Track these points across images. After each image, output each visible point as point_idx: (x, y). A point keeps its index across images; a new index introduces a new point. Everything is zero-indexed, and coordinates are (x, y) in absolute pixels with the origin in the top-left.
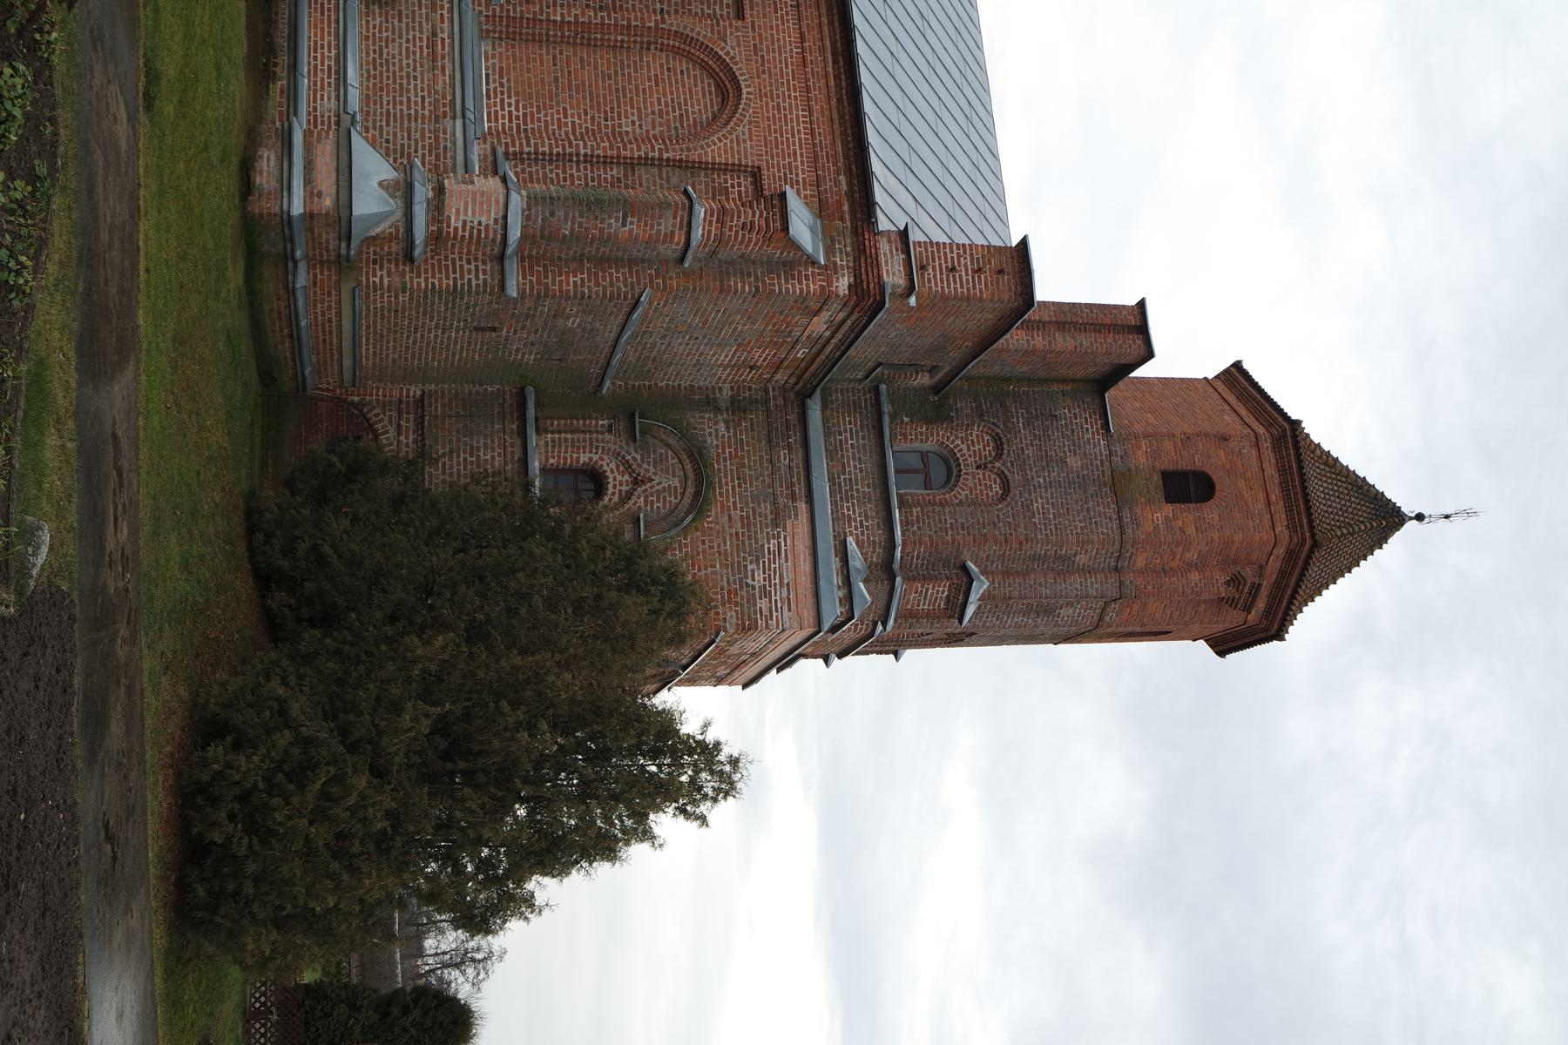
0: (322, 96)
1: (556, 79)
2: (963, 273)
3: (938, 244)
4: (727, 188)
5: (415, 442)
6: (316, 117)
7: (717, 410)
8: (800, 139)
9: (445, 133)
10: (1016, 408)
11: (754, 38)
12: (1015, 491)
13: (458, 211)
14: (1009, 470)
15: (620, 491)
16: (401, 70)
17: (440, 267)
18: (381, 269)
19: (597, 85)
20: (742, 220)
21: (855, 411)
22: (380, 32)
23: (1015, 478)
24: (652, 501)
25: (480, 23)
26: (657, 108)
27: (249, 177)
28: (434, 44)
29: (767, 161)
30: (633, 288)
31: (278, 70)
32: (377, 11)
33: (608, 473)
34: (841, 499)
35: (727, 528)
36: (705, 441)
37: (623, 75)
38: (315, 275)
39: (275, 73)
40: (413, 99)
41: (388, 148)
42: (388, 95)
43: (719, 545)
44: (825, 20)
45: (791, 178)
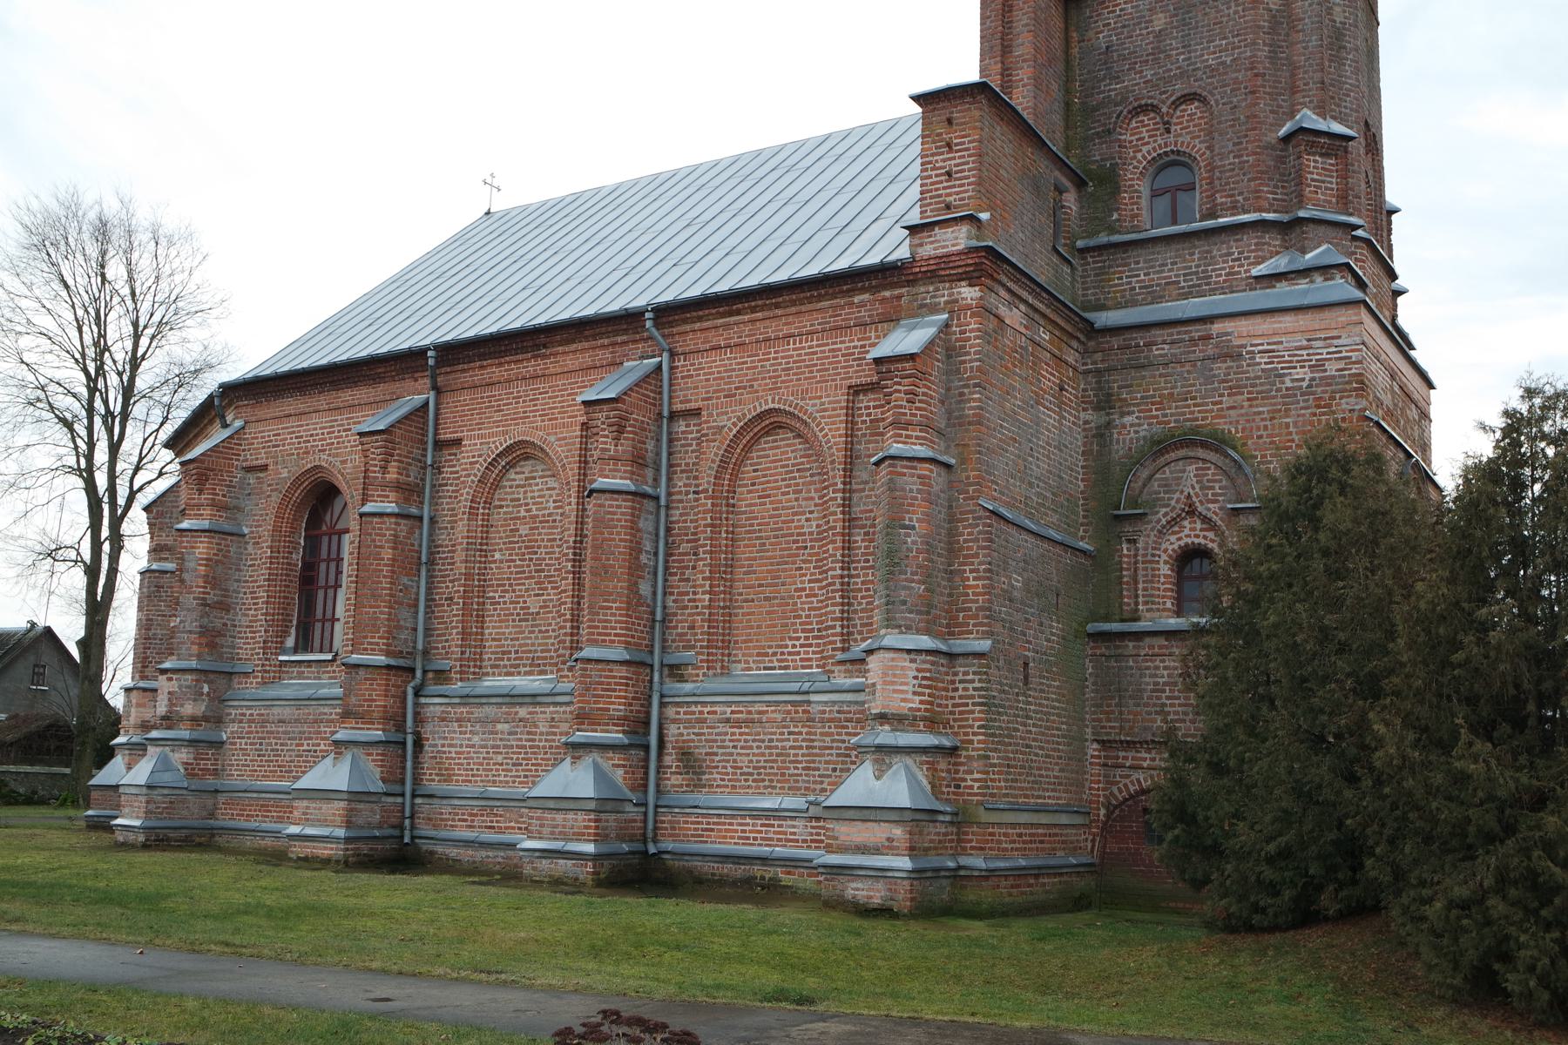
0: (792, 834)
1: (766, 599)
2: (953, 162)
3: (922, 193)
4: (871, 421)
5: (1149, 751)
6: (812, 841)
7: (1109, 424)
8: (818, 346)
9: (824, 712)
10: (1099, 93)
11: (718, 398)
12: (1195, 87)
13: (903, 700)
14: (1171, 96)
15: (1201, 530)
16: (763, 755)
17: (961, 720)
18: (965, 780)
19: (770, 558)
20: (905, 403)
21: (1107, 273)
22: (727, 774)
23: (1180, 88)
24: (1213, 495)
25: (715, 675)
26: (792, 496)
27: (875, 910)
29: (841, 379)
30: (980, 518)
31: (767, 876)
32: (707, 776)
33: (1182, 543)
34: (1207, 284)
35: (1243, 411)
36: (1145, 437)
37: (760, 531)
38: (972, 848)
39: (770, 879)
40: (791, 743)
41: (841, 770)
42: (789, 768)
43: (1262, 420)
44: (697, 326)
45: (859, 353)
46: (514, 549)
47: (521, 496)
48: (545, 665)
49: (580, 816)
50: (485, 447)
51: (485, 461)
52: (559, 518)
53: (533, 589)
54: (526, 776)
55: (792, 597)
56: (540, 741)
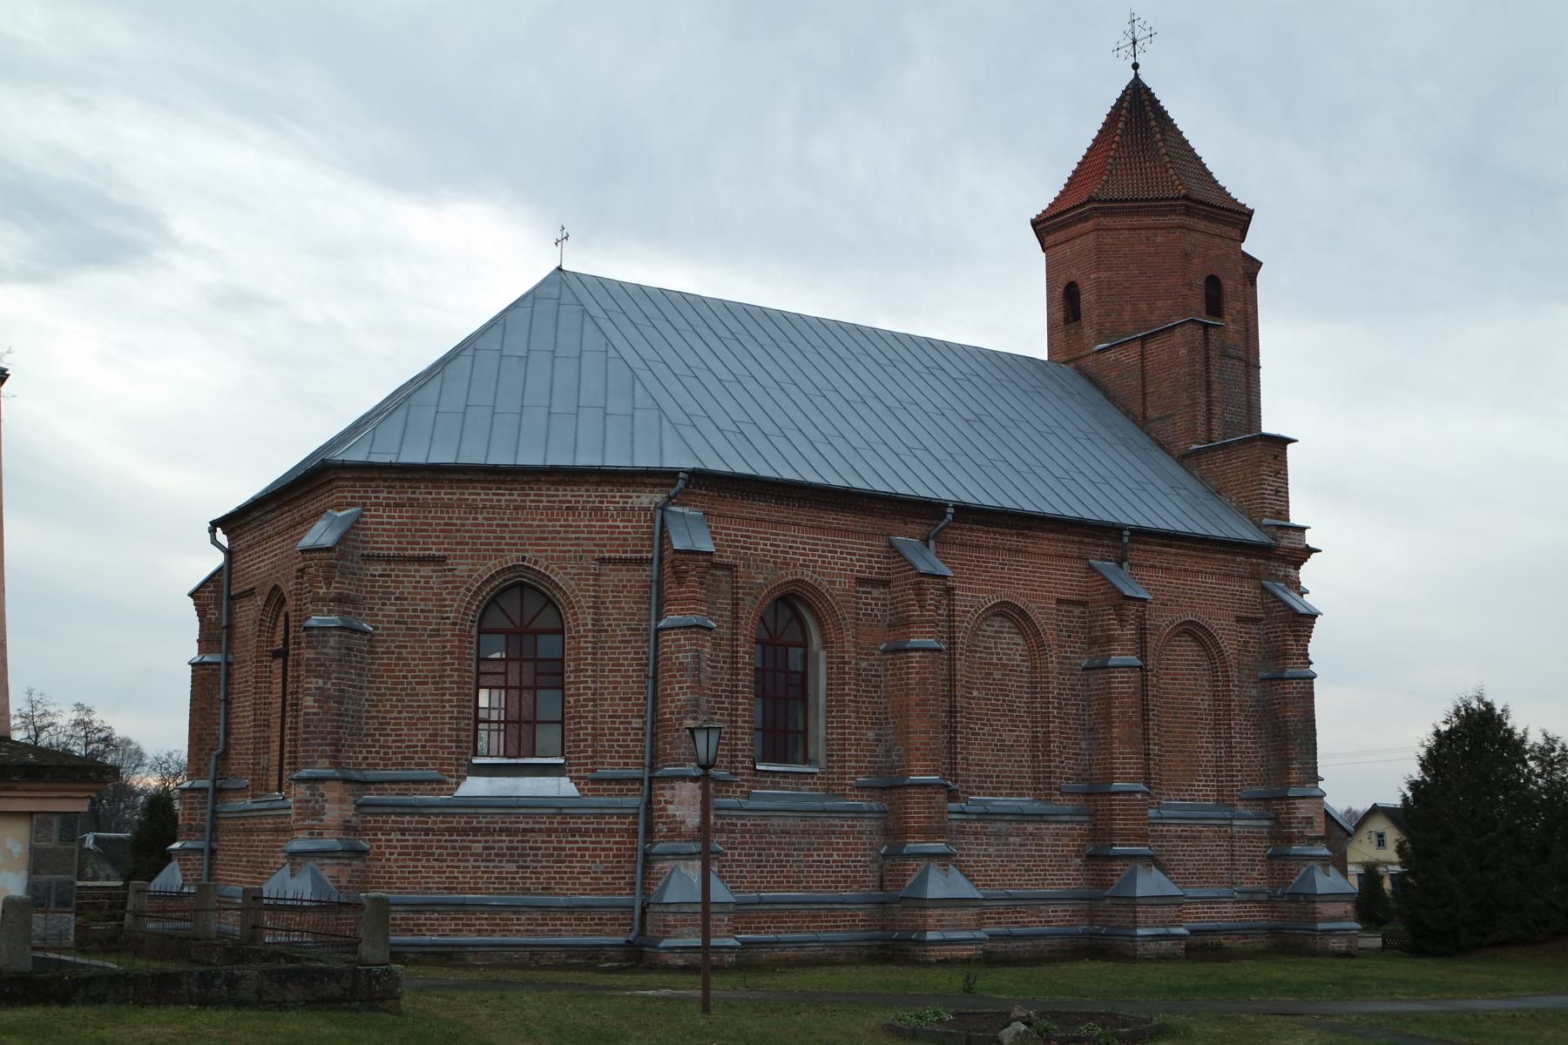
1: (1180, 751)
16: (1201, 860)
22: (1180, 874)
28: (1186, 837)
31: (1215, 942)
37: (1173, 703)
44: (1141, 546)
46: (989, 689)
47: (992, 645)
48: (1022, 789)
49: (1174, 909)
50: (977, 600)
51: (976, 611)
52: (1025, 669)
53: (1007, 725)
54: (1036, 880)
55: (1196, 752)
56: (1047, 851)
